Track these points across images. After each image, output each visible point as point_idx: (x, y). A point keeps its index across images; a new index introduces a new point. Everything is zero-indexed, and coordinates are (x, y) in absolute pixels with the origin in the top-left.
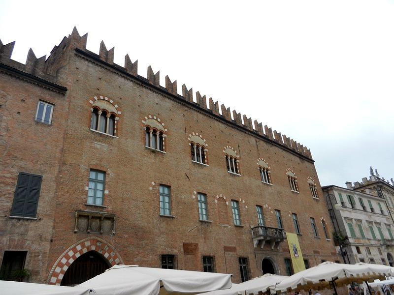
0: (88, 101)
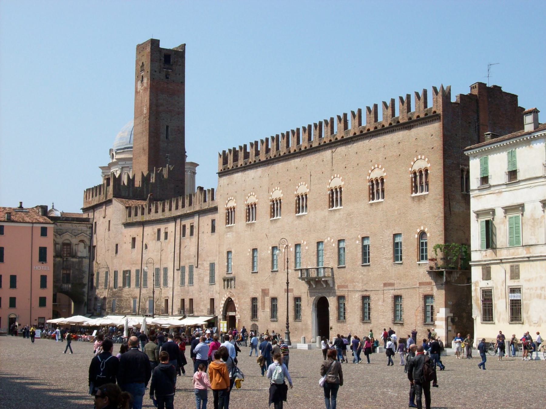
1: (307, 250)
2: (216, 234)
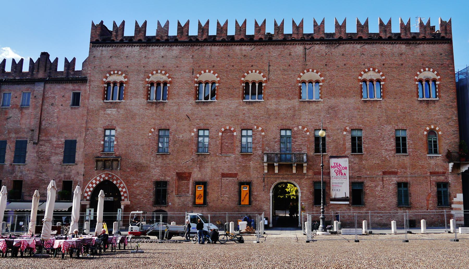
0: (102, 80)
1: (264, 136)
2: (80, 110)
